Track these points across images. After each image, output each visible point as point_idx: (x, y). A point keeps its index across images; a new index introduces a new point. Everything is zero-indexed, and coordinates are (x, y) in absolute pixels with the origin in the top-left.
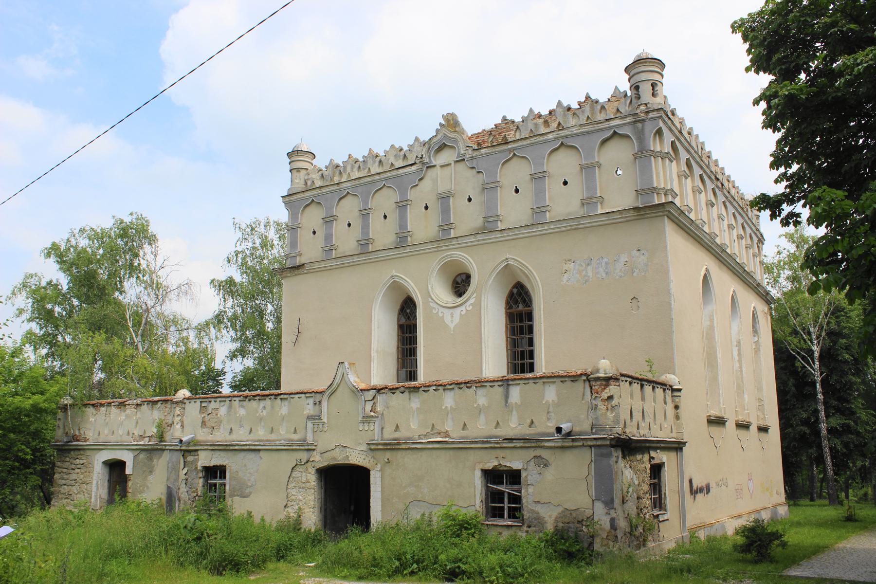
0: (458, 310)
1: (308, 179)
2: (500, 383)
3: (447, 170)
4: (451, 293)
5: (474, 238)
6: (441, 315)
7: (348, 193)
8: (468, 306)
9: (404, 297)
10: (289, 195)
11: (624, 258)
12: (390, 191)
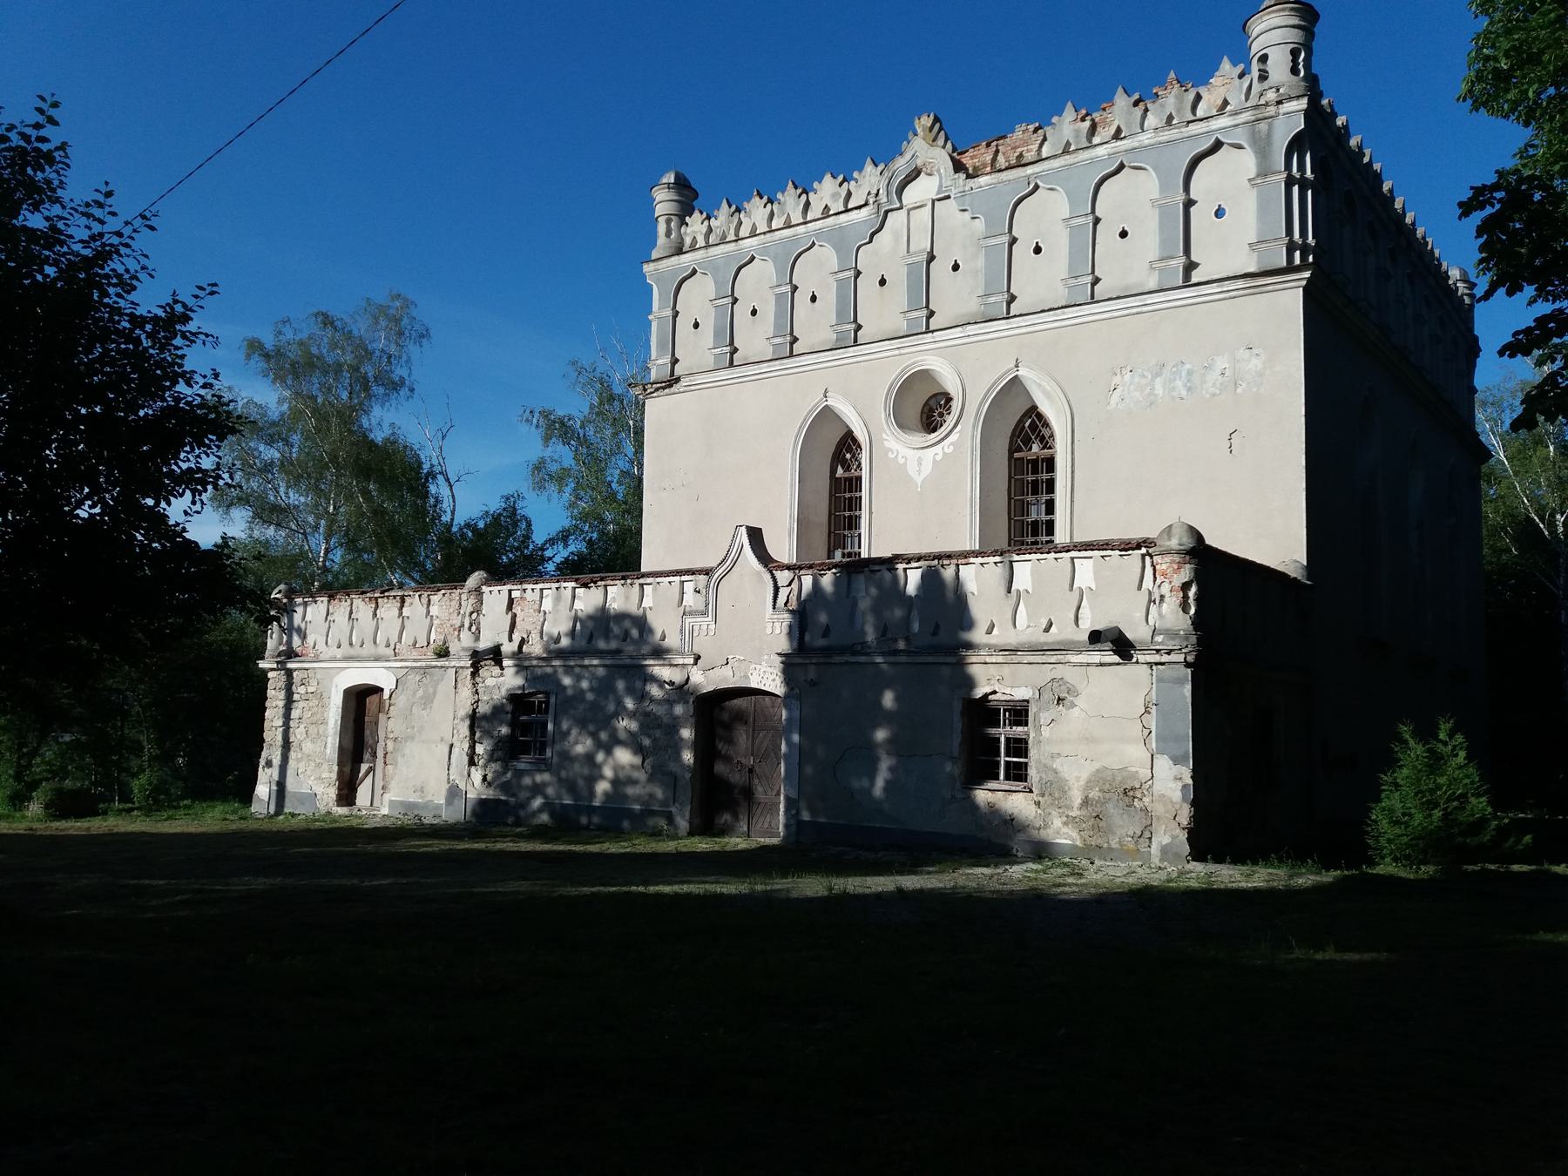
2: (998, 559)
5: (961, 332)
6: (901, 461)
11: (1221, 363)
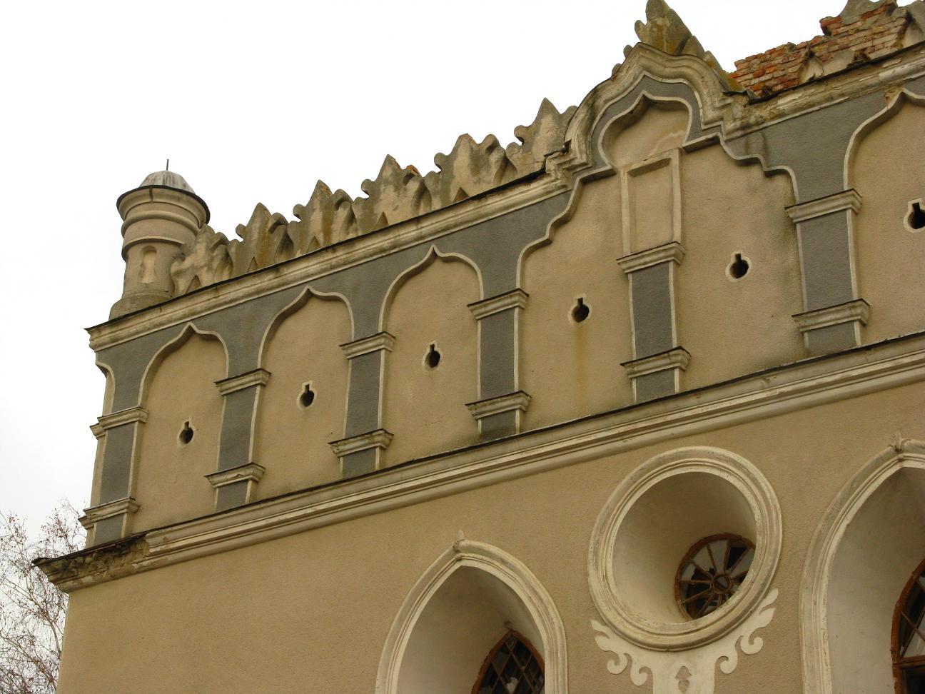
0: (707, 658)
1: (179, 273)
3: (654, 185)
4: (674, 609)
5: (763, 389)
6: (638, 679)
7: (310, 295)
8: (748, 638)
9: (498, 634)
10: (113, 322)
12: (457, 271)
